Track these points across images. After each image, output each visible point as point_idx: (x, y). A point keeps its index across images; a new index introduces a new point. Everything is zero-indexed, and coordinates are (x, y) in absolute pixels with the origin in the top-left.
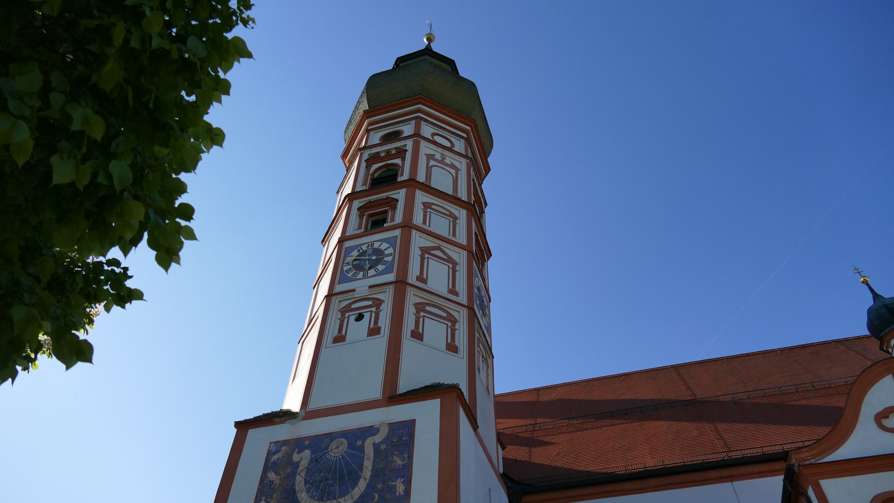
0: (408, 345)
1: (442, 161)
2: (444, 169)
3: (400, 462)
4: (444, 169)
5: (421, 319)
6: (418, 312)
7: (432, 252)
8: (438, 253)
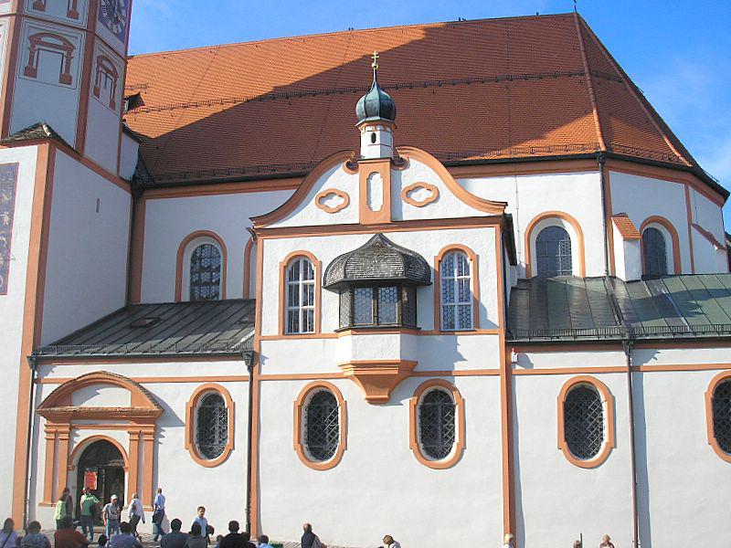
0: (21, 82)
3: (6, 198)
5: (36, 54)
6: (33, 46)
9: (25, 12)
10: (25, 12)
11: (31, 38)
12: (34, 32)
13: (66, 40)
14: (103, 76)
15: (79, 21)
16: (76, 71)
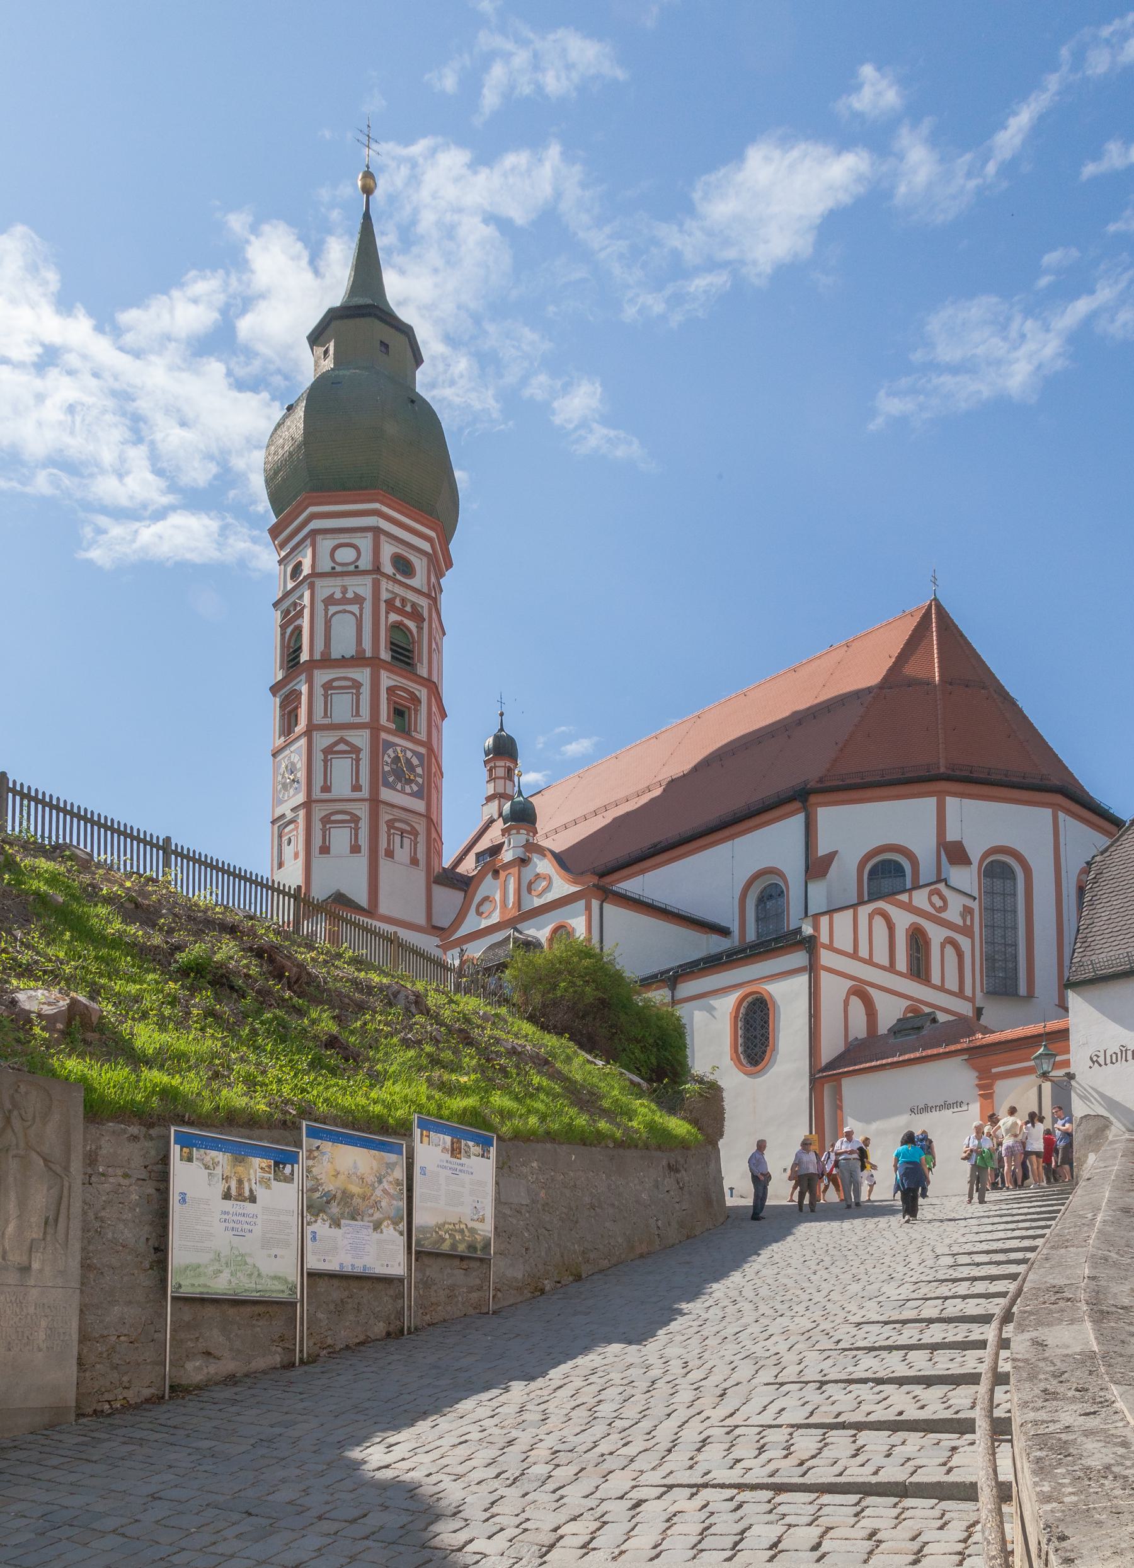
1: (344, 601)
2: (345, 611)
4: (345, 611)
7: (337, 748)
8: (342, 747)
9: (314, 797)
10: (314, 797)
11: (322, 820)
12: (323, 814)
13: (351, 813)
14: (398, 839)
15: (363, 793)
16: (364, 841)
